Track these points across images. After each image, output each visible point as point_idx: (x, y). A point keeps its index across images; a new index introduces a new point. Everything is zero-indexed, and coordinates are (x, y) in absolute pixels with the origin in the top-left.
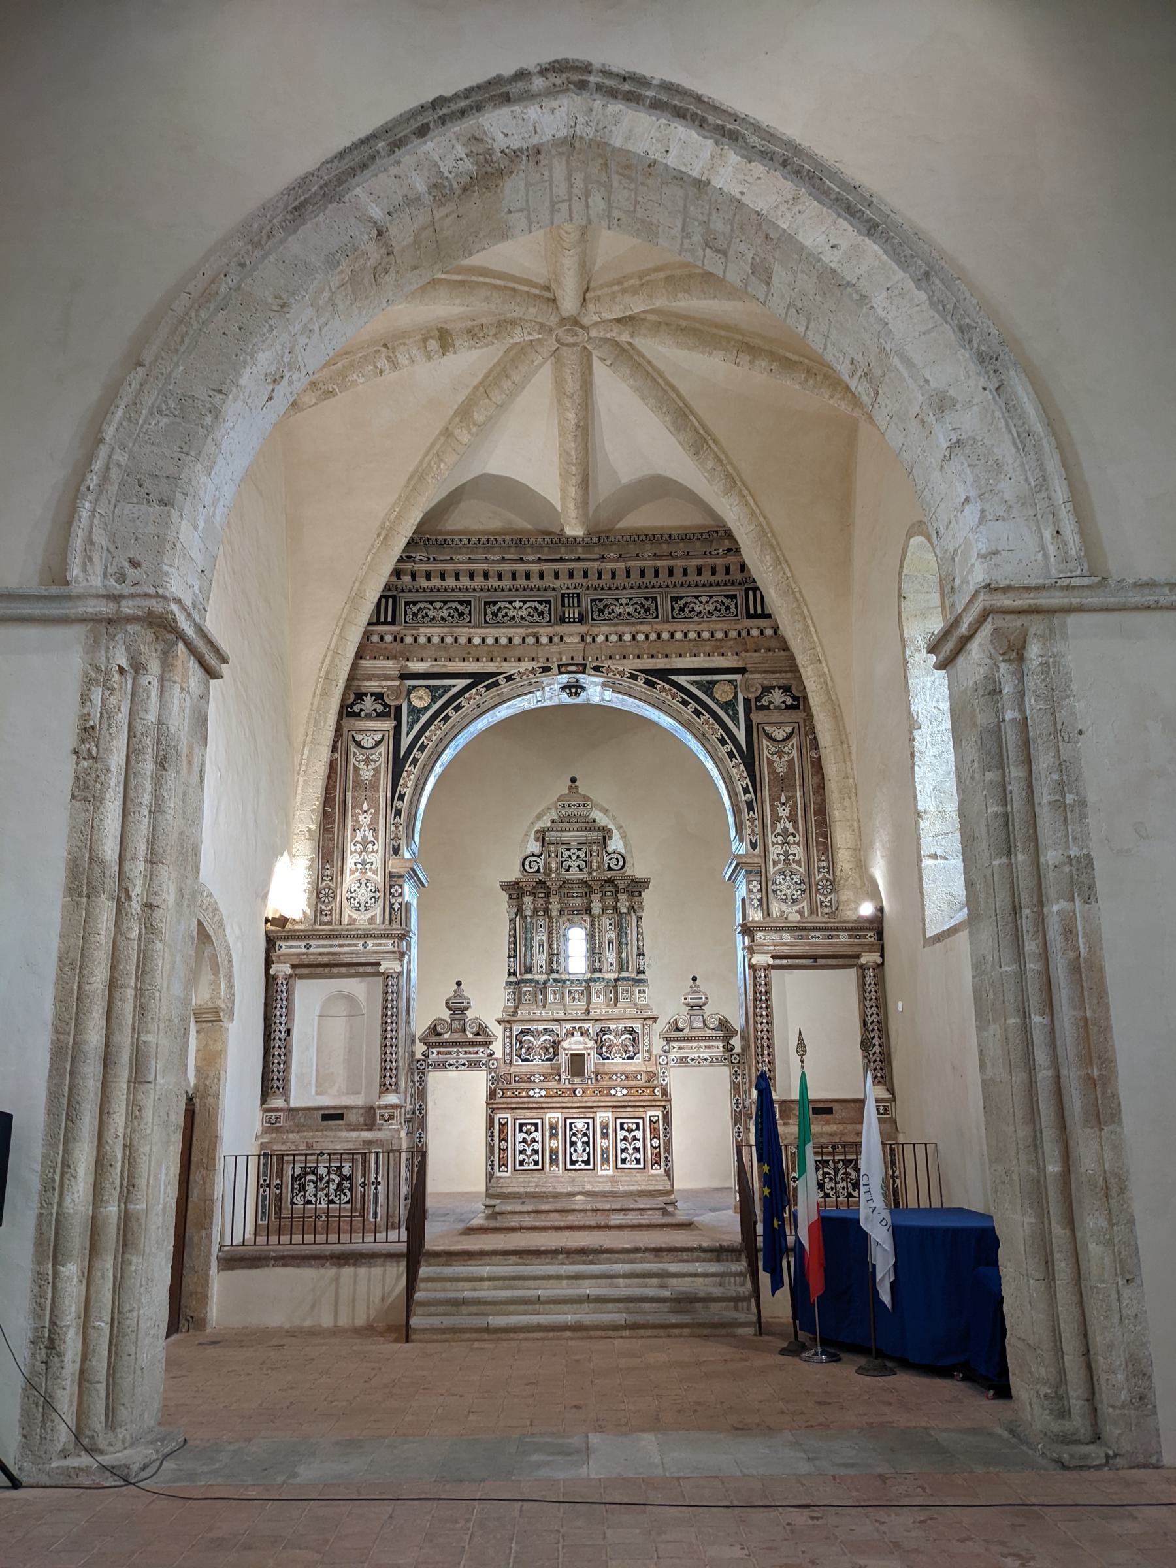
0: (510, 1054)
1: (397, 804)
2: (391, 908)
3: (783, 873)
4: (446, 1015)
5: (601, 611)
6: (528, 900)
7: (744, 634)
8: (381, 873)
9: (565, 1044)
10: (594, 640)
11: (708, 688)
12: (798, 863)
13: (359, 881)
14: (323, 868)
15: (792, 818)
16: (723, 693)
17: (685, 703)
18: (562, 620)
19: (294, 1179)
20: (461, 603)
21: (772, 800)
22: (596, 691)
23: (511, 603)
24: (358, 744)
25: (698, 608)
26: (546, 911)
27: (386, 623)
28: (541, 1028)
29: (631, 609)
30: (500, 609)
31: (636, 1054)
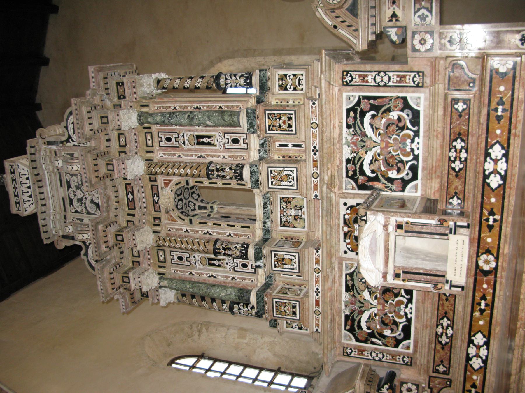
28: (346, 296)
31: (406, 105)
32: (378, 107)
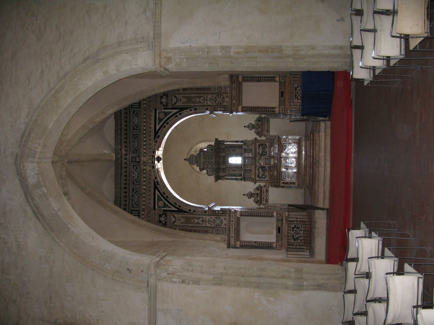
0: (264, 180)
1: (192, 211)
2: (222, 214)
3: (215, 101)
4: (252, 199)
5: (137, 150)
6: (220, 174)
7: (145, 109)
8: (212, 217)
9: (262, 165)
10: (145, 153)
11: (160, 120)
12: (213, 96)
13: (214, 223)
14: (210, 233)
15: (200, 97)
16: (162, 116)
17: (165, 127)
18: (139, 162)
19: (295, 240)
20: (133, 191)
21: (194, 103)
22: (159, 153)
23: (133, 177)
24: (174, 222)
25: (137, 122)
26: (224, 169)
27: (139, 213)
28: (257, 172)
29: (136, 142)
30: (135, 180)
31: (265, 145)
32: (262, 145)
